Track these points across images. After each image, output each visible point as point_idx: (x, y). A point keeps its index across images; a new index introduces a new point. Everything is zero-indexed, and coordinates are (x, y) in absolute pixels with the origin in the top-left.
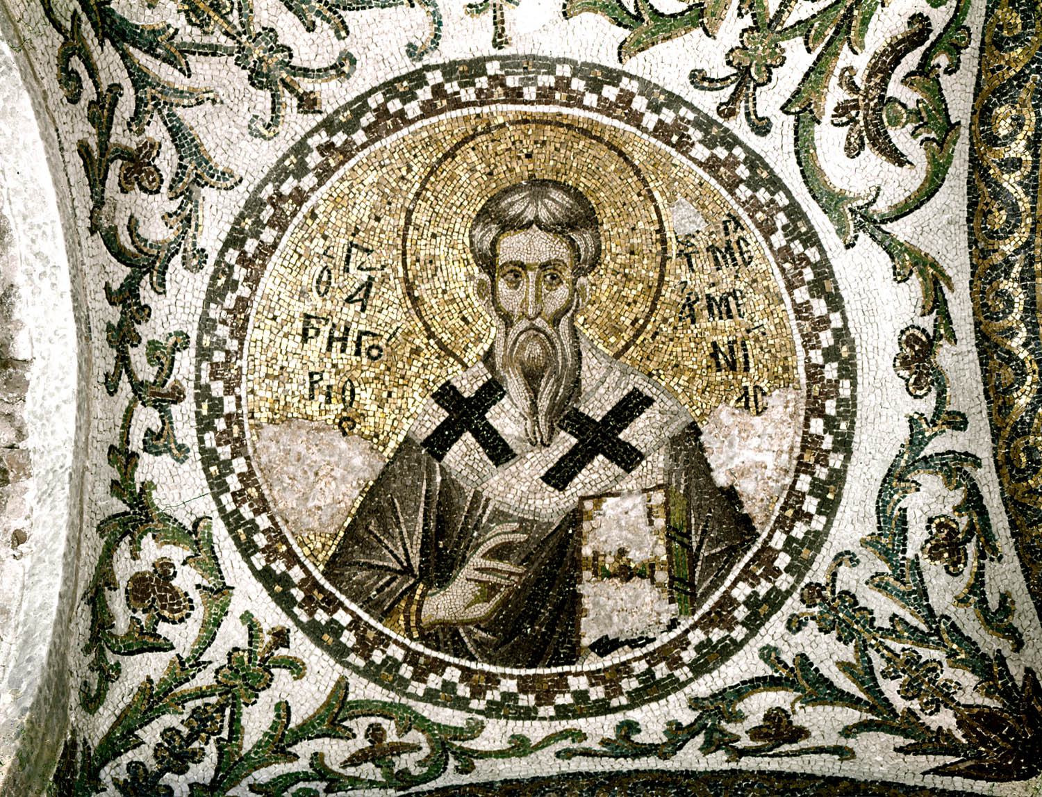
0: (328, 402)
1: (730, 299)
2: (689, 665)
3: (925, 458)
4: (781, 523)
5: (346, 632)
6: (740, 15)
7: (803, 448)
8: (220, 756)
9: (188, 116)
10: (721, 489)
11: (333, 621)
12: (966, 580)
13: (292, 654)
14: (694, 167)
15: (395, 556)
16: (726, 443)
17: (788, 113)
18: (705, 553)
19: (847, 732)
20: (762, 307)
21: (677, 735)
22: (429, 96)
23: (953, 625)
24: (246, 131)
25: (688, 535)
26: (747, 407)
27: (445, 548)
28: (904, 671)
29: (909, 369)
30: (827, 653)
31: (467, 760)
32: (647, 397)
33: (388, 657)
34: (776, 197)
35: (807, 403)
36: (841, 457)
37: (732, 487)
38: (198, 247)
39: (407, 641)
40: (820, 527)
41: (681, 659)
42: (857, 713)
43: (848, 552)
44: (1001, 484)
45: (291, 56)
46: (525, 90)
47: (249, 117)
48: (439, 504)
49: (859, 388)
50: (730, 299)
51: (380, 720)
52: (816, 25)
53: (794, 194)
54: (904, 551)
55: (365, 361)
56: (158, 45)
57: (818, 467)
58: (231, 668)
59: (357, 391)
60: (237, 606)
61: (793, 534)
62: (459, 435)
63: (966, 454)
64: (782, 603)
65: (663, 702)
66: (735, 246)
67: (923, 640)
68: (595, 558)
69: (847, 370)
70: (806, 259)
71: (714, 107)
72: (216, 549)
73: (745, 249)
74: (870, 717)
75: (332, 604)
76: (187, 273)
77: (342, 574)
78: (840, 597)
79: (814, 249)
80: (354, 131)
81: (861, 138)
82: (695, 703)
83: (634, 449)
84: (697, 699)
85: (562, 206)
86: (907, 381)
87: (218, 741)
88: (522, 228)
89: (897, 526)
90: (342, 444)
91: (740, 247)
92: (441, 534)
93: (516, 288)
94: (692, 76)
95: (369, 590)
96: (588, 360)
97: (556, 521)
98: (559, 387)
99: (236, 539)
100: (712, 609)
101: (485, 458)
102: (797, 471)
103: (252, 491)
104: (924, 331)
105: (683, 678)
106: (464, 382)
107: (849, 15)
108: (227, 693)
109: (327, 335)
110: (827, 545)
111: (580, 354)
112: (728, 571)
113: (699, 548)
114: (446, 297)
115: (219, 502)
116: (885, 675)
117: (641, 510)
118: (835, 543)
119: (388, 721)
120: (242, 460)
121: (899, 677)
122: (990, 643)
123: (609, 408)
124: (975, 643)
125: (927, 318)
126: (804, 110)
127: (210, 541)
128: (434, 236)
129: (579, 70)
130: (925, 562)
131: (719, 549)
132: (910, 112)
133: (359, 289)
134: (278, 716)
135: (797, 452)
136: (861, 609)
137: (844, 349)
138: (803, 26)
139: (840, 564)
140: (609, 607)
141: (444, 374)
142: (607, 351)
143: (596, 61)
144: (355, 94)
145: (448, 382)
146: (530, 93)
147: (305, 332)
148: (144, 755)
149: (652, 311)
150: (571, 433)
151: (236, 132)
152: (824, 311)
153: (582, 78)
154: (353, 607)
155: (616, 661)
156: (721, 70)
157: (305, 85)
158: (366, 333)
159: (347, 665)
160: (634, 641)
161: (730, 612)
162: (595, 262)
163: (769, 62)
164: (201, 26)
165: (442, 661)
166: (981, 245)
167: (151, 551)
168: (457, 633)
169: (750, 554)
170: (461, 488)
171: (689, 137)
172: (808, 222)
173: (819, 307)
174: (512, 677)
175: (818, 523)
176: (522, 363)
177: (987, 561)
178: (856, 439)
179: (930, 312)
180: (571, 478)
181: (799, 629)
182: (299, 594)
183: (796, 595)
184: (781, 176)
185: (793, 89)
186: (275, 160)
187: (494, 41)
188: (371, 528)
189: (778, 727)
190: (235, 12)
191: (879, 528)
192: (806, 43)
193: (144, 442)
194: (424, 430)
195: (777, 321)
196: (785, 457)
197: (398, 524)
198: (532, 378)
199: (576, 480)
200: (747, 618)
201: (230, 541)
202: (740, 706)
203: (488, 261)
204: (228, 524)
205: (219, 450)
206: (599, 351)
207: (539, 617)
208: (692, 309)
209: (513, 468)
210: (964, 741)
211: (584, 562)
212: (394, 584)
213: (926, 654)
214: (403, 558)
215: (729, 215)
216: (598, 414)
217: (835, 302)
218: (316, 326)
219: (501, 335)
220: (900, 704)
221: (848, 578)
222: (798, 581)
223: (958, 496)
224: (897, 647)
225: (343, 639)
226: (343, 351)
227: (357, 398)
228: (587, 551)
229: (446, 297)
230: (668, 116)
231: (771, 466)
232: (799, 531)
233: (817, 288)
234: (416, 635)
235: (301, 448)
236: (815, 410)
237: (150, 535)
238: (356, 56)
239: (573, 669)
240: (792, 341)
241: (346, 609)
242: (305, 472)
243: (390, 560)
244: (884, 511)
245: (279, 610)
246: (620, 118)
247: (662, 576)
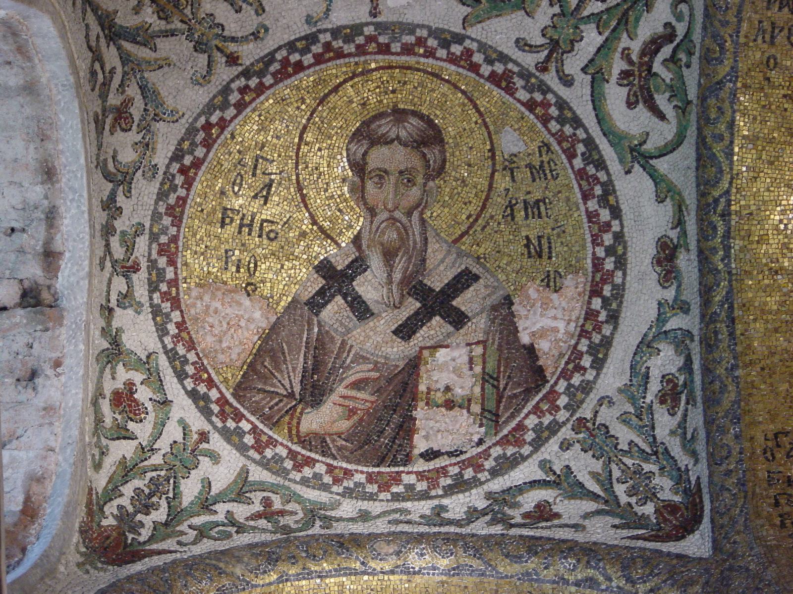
0: (238, 271)
1: (541, 204)
2: (488, 471)
3: (665, 332)
4: (565, 375)
5: (247, 436)
7: (586, 319)
8: (169, 507)
9: (153, 77)
10: (524, 346)
11: (238, 427)
12: (678, 419)
13: (212, 448)
14: (518, 105)
15: (283, 385)
16: (532, 312)
17: (586, 73)
18: (508, 393)
19: (586, 516)
20: (564, 212)
21: (473, 514)
22: (320, 50)
23: (666, 449)
24: (189, 81)
25: (497, 379)
26: (548, 286)
27: (318, 380)
28: (631, 479)
29: (661, 266)
30: (584, 466)
31: (328, 521)
32: (475, 275)
33: (276, 454)
34: (578, 132)
35: (592, 286)
36: (611, 327)
37: (532, 345)
38: (153, 163)
39: (290, 444)
40: (591, 378)
41: (483, 465)
42: (596, 505)
43: (608, 397)
45: (223, 30)
46: (393, 45)
47: (192, 72)
48: (316, 348)
49: (628, 278)
50: (541, 204)
51: (270, 494)
52: (605, 17)
53: (590, 131)
54: (644, 397)
55: (265, 242)
56: (139, 36)
57: (594, 334)
58: (172, 454)
59: (259, 263)
60: (176, 413)
61: (572, 382)
62: (333, 296)
64: (558, 430)
65: (467, 494)
66: (546, 165)
68: (428, 393)
69: (620, 262)
70: (597, 179)
71: (533, 64)
72: (161, 375)
73: (553, 168)
74: (604, 507)
75: (238, 417)
76: (145, 182)
77: (245, 396)
78: (598, 428)
79: (603, 172)
80: (264, 76)
81: (637, 97)
82: (489, 495)
83: (463, 313)
84: (490, 493)
85: (418, 129)
86: (659, 275)
87: (167, 498)
88: (387, 143)
90: (247, 302)
91: (550, 166)
92: (315, 370)
93: (380, 188)
94: (517, 41)
95: (264, 407)
96: (433, 246)
97: (401, 364)
98: (410, 263)
99: (174, 368)
100: (510, 432)
101: (351, 315)
102: (580, 336)
103: (184, 335)
104: (672, 240)
105: (483, 479)
106: (338, 258)
107: (625, 13)
108: (171, 469)
109: (238, 222)
110: (594, 391)
111: (426, 239)
112: (523, 407)
113: (505, 389)
114: (327, 194)
115: (162, 342)
116: (618, 481)
117: (466, 359)
118: (600, 390)
119: (276, 496)
120: (178, 313)
121: (627, 482)
122: (683, 460)
123: (446, 282)
124: (676, 461)
125: (674, 231)
126: (597, 73)
127: (157, 369)
128: (320, 149)
129: (435, 33)
130: (656, 406)
131: (519, 390)
132: (667, 85)
133: (263, 189)
134: (203, 487)
135: (581, 321)
137: (620, 248)
138: (597, 19)
140: (435, 429)
141: (323, 251)
142: (447, 238)
143: (446, 27)
144: (267, 51)
145: (325, 259)
146: (396, 47)
147: (223, 219)
148: (125, 501)
149: (484, 207)
150: (417, 299)
151: (182, 82)
152: (608, 218)
153: (435, 38)
154: (253, 419)
155: (438, 466)
157: (232, 47)
158: (267, 221)
159: (248, 458)
160: (451, 452)
161: (522, 435)
162: (441, 170)
163: (572, 38)
164: (166, 19)
165: (313, 459)
167: (123, 375)
168: (324, 438)
169: (540, 395)
170: (333, 338)
171: (514, 84)
172: (599, 152)
173: (605, 215)
174: (362, 472)
175: (590, 375)
176: (382, 244)
177: (690, 406)
178: (623, 315)
179: (676, 227)
180: (414, 333)
181: (568, 449)
182: (216, 408)
183: (569, 426)
184: (581, 117)
185: (590, 57)
186: (207, 100)
187: (370, 12)
188: (266, 364)
189: (542, 512)
190: (189, 7)
191: (631, 381)
192: (598, 28)
193: (118, 301)
194: (306, 293)
195: (574, 222)
196: (573, 324)
197: (285, 361)
198: (389, 255)
199: (418, 335)
200: (533, 440)
201: (170, 370)
202: (520, 499)
203: (359, 167)
204: (169, 358)
205: (163, 305)
206: (441, 238)
207: (385, 434)
208: (512, 210)
209: (371, 324)
210: (655, 521)
211: (420, 396)
212: (281, 404)
213: (647, 467)
214: (288, 386)
215: (543, 142)
216: (438, 286)
217: (616, 212)
218: (231, 215)
219: (368, 223)
220: (624, 499)
221: (607, 415)
222: (571, 416)
223: (680, 361)
224: (629, 462)
225: (245, 440)
226: (249, 234)
227: (259, 269)
228: (422, 388)
229: (327, 194)
230: (499, 68)
231: (562, 331)
232: (576, 380)
233: (604, 200)
234: (296, 440)
235: (217, 304)
236: (595, 292)
237: (121, 363)
238: (269, 26)
239: (406, 469)
240: (584, 239)
241: (248, 420)
242: (221, 322)
243: (278, 387)
244: (635, 369)
245: (202, 418)
246: (463, 67)
247: (476, 408)
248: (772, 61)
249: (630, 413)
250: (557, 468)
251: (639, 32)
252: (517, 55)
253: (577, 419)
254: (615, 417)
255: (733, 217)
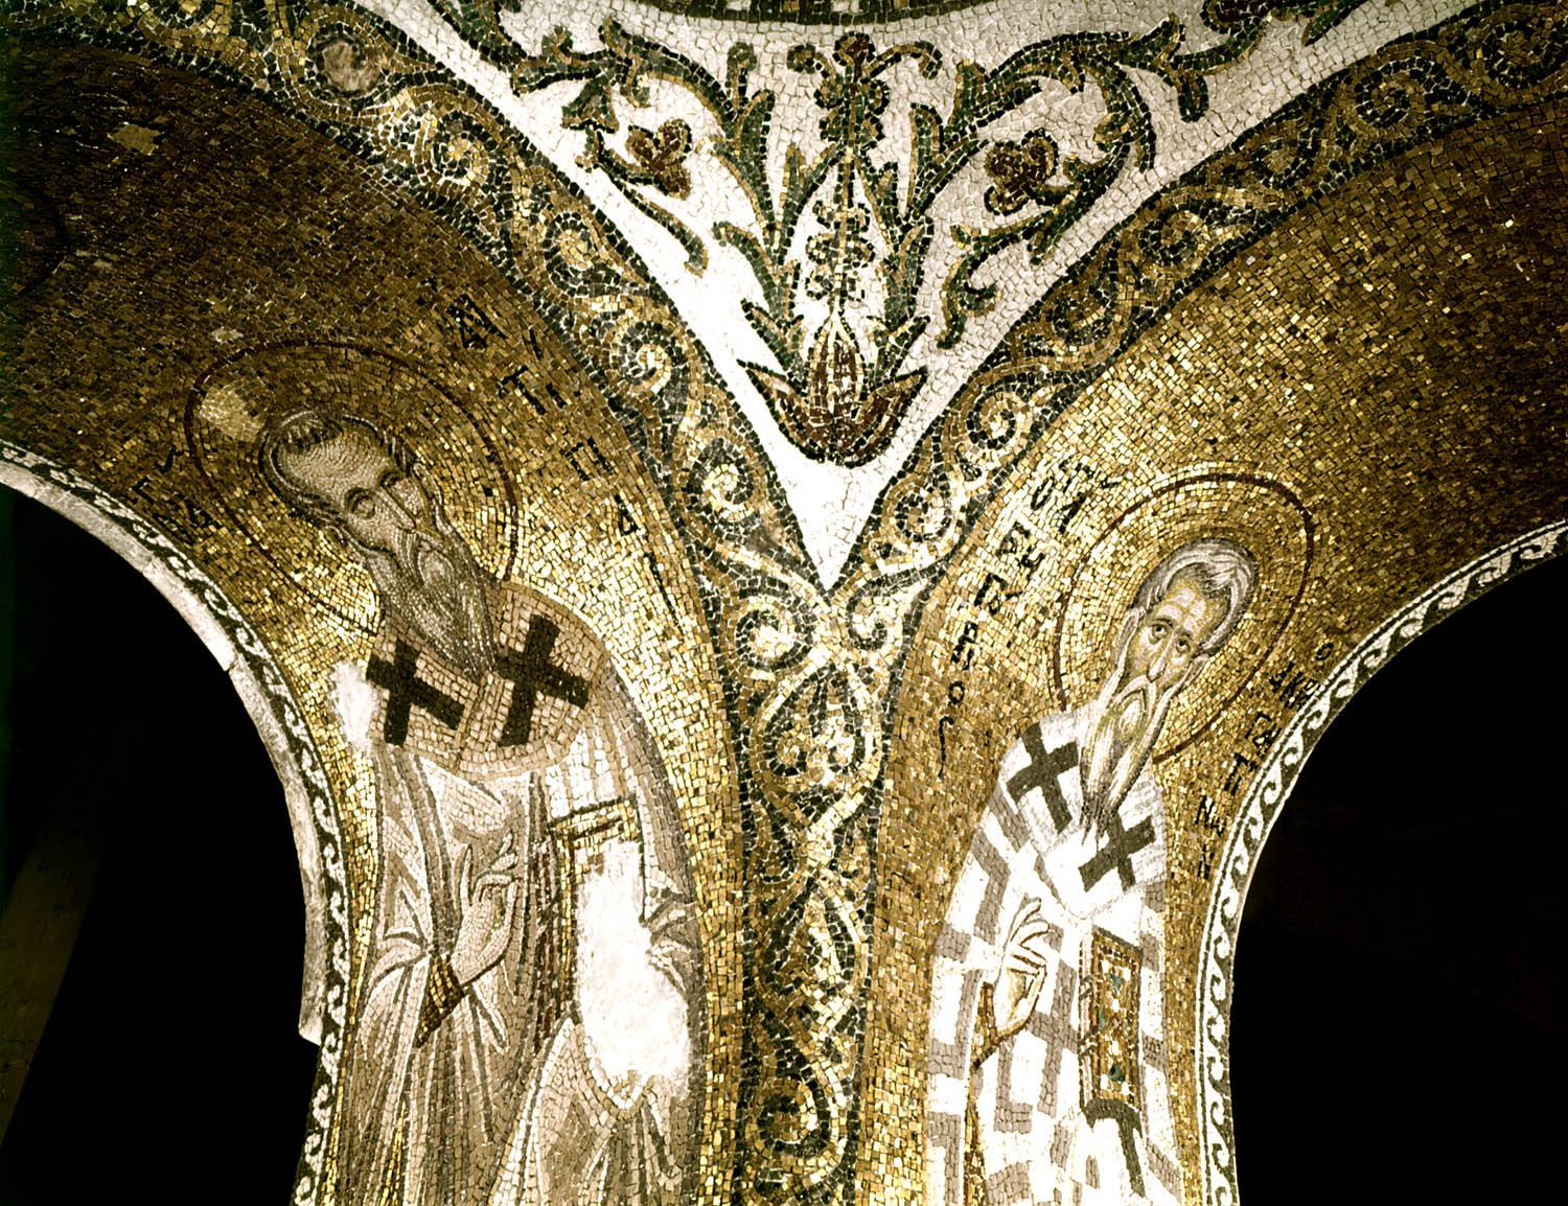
28: (837, 225)
43: (938, 55)
44: (1130, 218)
54: (982, 124)
63: (1153, 137)
64: (815, 21)
67: (890, 218)
78: (874, 86)
89: (1010, 94)
122: (931, 301)
136: (875, 121)
139: (916, 56)
166: (1472, 35)
181: (799, 69)
191: (994, 73)
220: (797, 252)
221: (906, 83)
222: (859, 20)
223: (1091, 155)
249: (939, 120)
250: (755, 82)
253: (861, 36)
254: (915, 98)
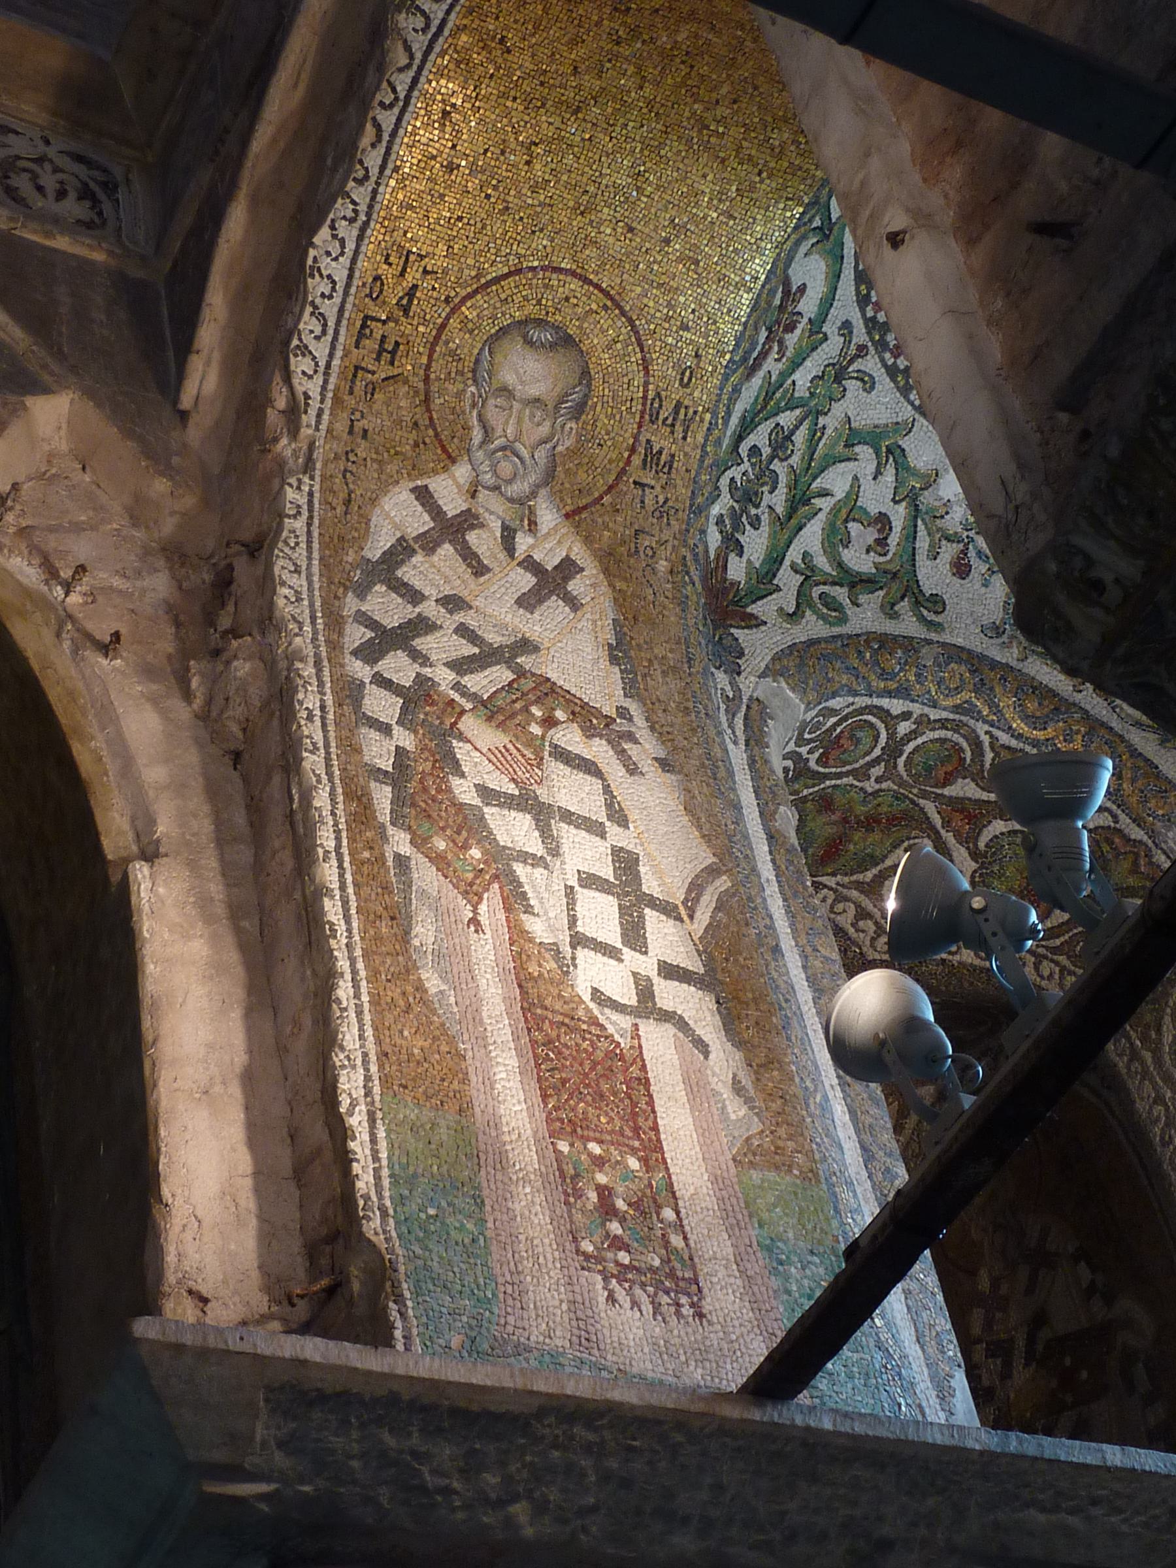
6: (824, 427)
94: (872, 388)
156: (852, 385)
248: (686, 380)
251: (760, 382)
252: (879, 373)
255: (806, 201)
